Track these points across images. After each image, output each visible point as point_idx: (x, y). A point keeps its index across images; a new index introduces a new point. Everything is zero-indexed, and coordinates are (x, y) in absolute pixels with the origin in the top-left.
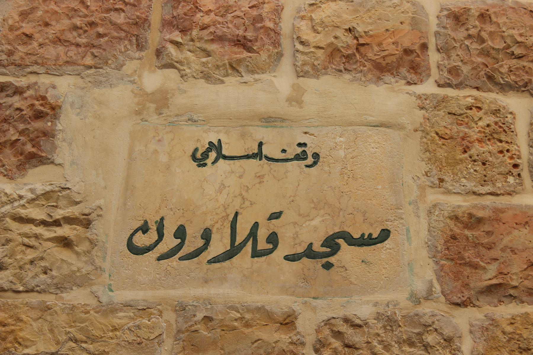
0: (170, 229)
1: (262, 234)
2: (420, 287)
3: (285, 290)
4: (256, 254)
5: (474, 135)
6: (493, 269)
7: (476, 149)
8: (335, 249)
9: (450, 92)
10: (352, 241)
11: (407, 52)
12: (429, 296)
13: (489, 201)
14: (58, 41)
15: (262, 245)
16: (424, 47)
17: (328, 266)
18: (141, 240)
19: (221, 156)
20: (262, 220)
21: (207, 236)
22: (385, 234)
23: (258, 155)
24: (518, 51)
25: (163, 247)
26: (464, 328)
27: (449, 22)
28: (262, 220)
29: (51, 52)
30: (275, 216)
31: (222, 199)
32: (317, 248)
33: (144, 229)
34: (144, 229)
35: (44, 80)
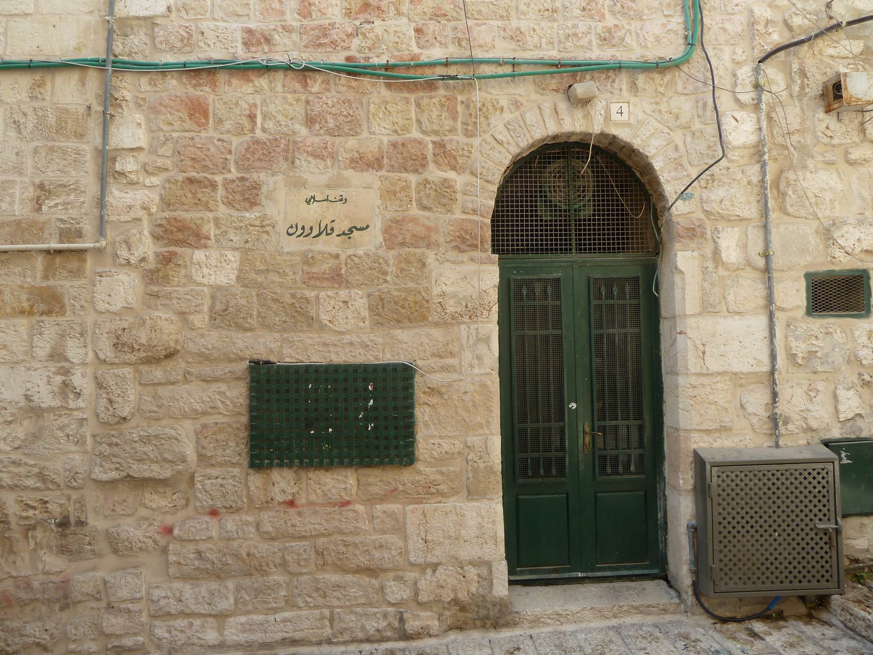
0: (300, 227)
1: (329, 228)
2: (378, 244)
3: (336, 246)
4: (327, 234)
5: (398, 189)
6: (401, 237)
7: (399, 195)
8: (352, 232)
9: (390, 174)
10: (357, 229)
11: (377, 159)
12: (381, 246)
13: (401, 214)
14: (260, 160)
15: (329, 232)
16: (383, 157)
17: (349, 238)
18: (291, 231)
19: (315, 200)
20: (329, 223)
21: (311, 229)
22: (368, 227)
23: (327, 200)
24: (414, 157)
25: (298, 233)
26: (391, 257)
27: (391, 148)
28: (329, 223)
29: (258, 164)
30: (333, 221)
31: (316, 216)
32: (346, 232)
33: (292, 227)
34: (292, 227)
35: (255, 176)
